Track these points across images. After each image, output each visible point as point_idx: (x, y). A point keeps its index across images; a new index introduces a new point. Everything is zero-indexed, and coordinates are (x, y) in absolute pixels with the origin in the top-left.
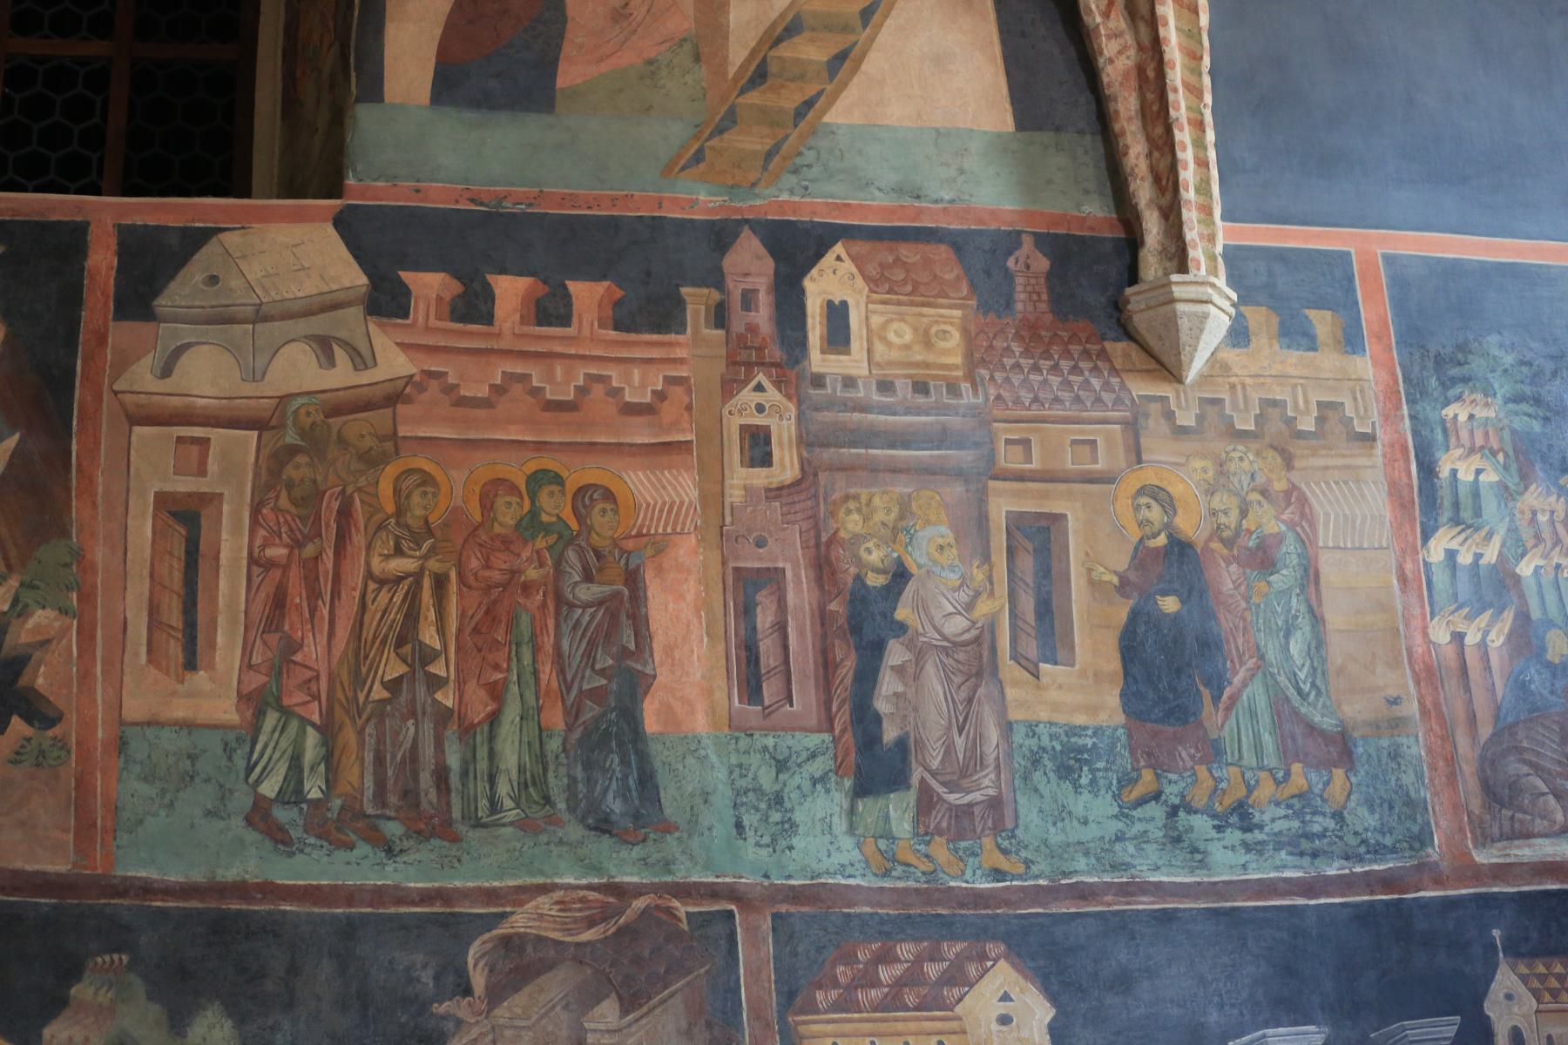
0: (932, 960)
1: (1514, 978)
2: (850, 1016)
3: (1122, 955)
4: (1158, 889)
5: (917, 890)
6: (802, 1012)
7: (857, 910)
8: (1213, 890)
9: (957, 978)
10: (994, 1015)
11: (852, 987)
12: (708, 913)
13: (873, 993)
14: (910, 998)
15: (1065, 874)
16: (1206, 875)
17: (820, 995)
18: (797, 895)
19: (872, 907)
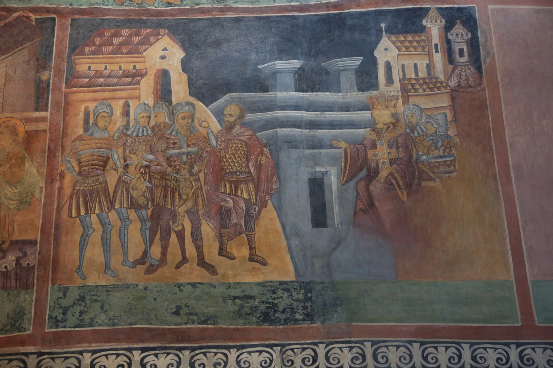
0: (136, 35)
1: (389, 42)
2: (98, 56)
3: (217, 34)
4: (237, 10)
5: (134, 10)
6: (78, 55)
7: (107, 17)
8: (260, 10)
9: (146, 42)
10: (160, 55)
11: (100, 46)
12: (44, 18)
13: (110, 48)
14: (124, 50)
15: (197, 4)
16: (257, 5)
17: (87, 49)
18: (82, 12)
19: (114, 16)
